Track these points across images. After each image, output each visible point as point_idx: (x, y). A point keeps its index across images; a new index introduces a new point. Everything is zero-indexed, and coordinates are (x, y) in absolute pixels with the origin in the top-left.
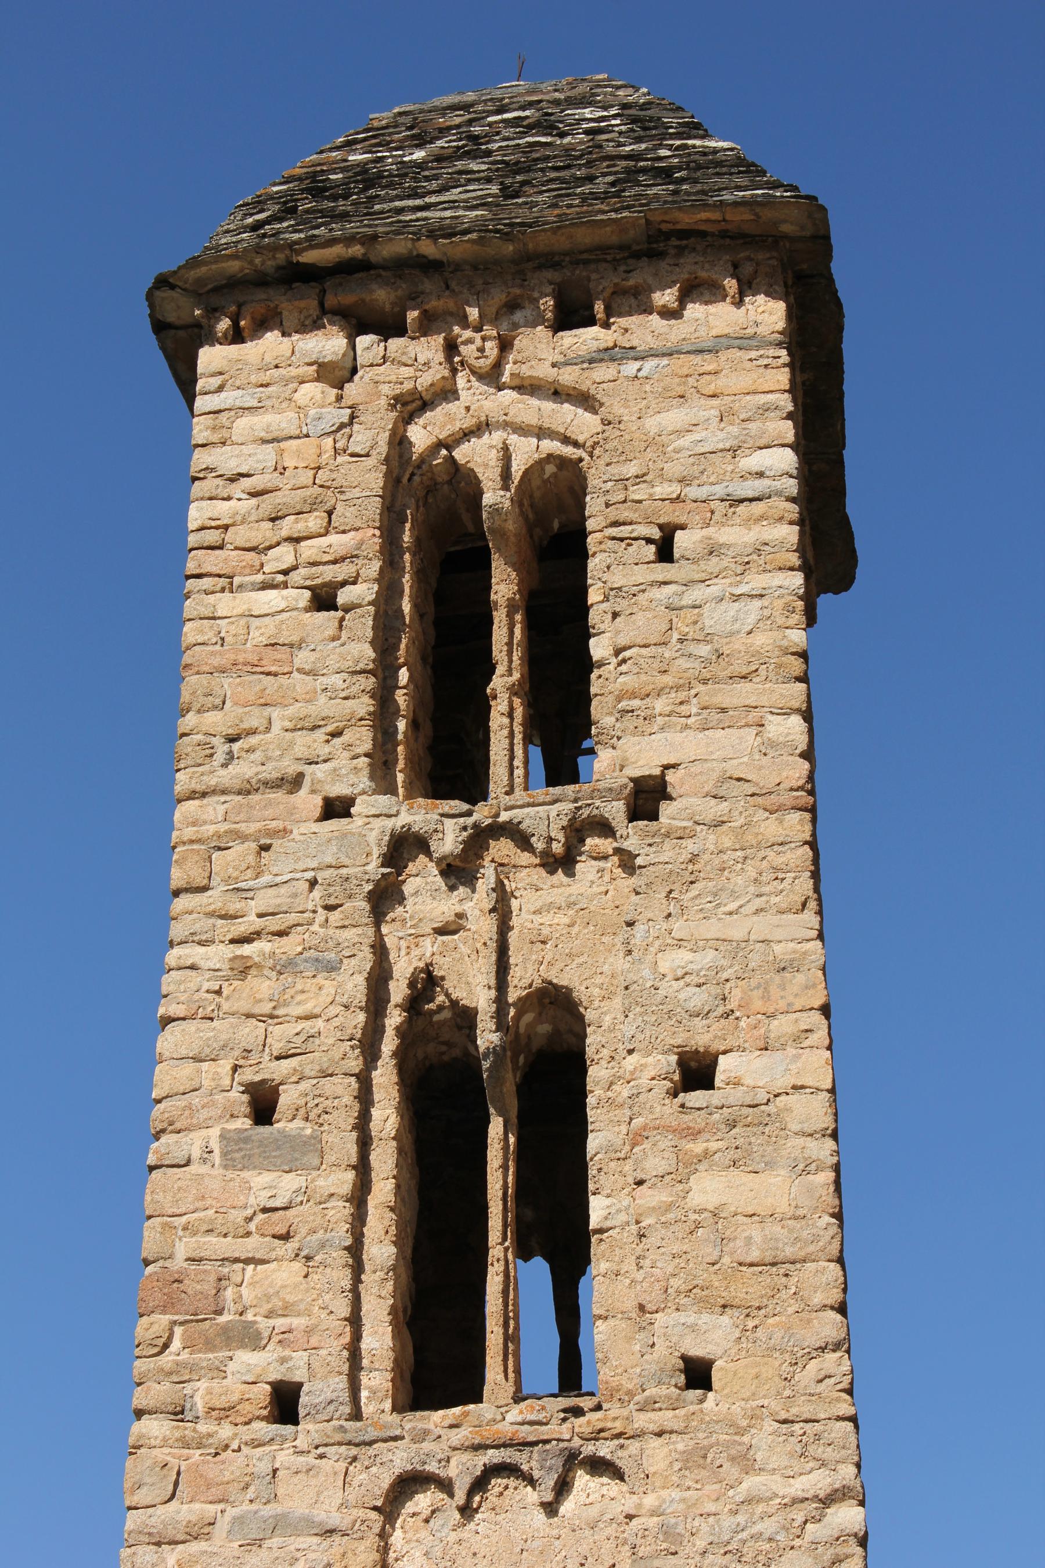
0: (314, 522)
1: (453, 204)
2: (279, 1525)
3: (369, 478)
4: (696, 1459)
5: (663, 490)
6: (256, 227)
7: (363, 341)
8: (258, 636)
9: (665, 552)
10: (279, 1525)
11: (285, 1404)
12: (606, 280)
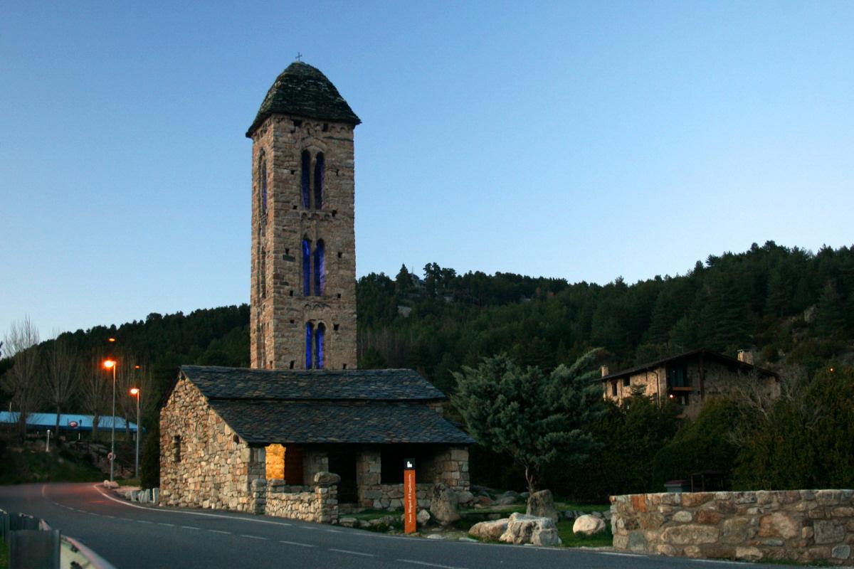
0: (291, 159)
1: (310, 106)
2: (292, 309)
3: (298, 153)
4: (339, 307)
5: (338, 164)
6: (281, 101)
7: (297, 128)
8: (284, 177)
9: (337, 175)
10: (292, 309)
11: (291, 293)
12: (330, 125)
